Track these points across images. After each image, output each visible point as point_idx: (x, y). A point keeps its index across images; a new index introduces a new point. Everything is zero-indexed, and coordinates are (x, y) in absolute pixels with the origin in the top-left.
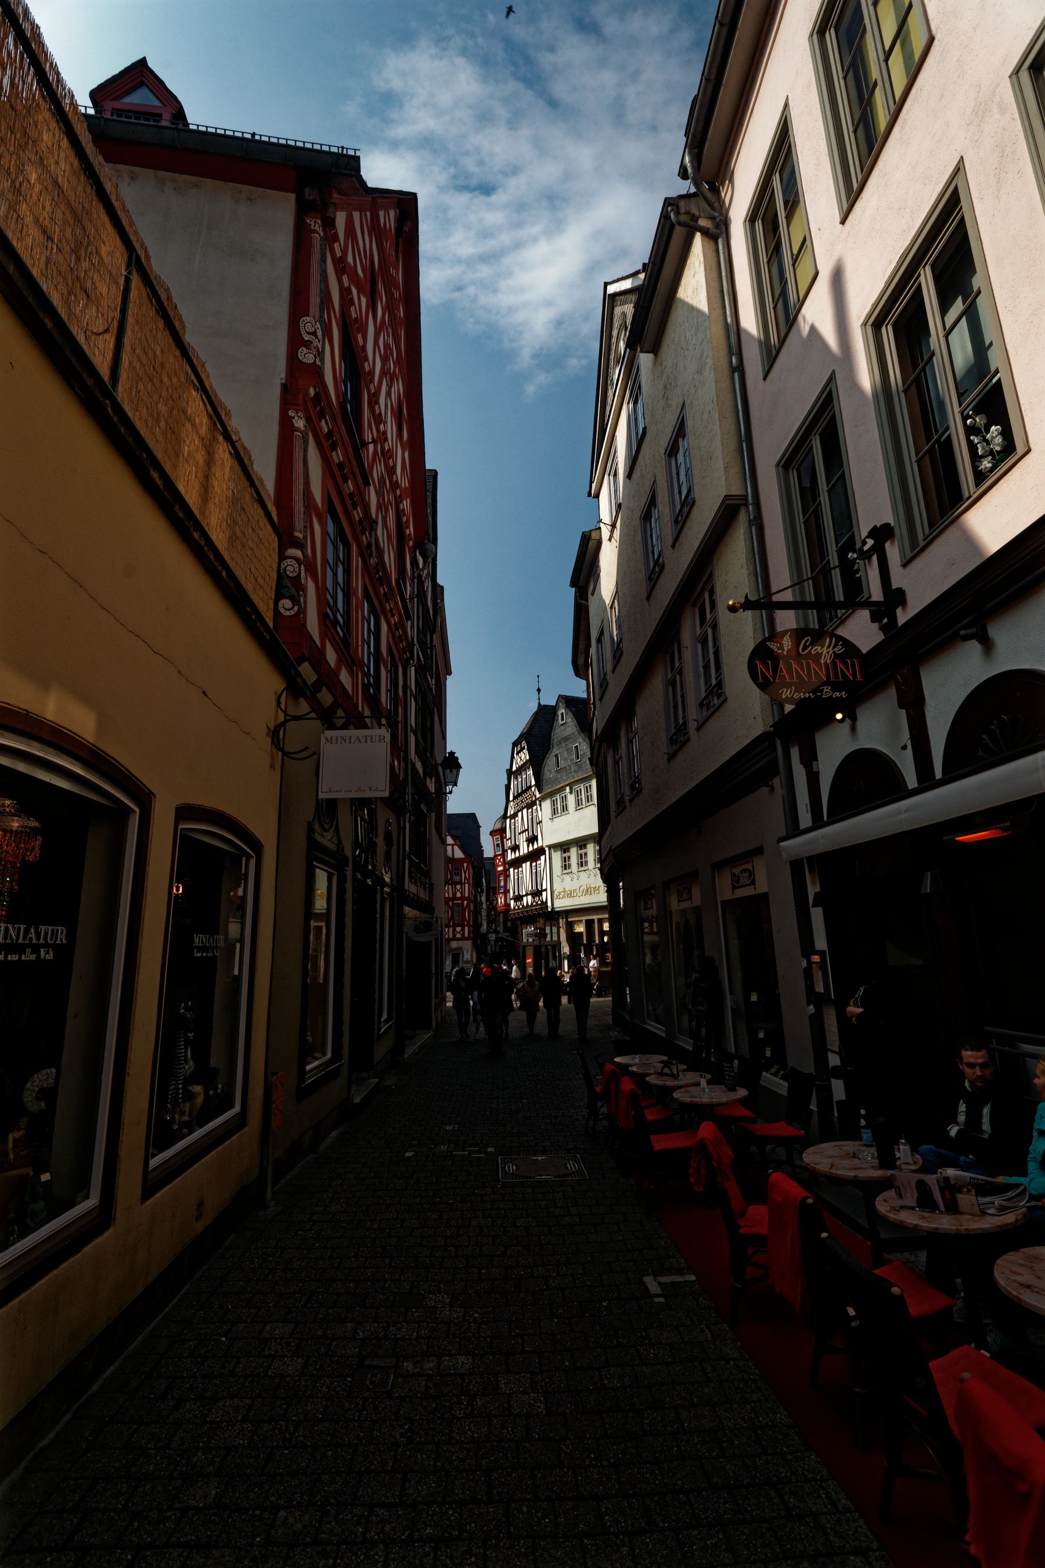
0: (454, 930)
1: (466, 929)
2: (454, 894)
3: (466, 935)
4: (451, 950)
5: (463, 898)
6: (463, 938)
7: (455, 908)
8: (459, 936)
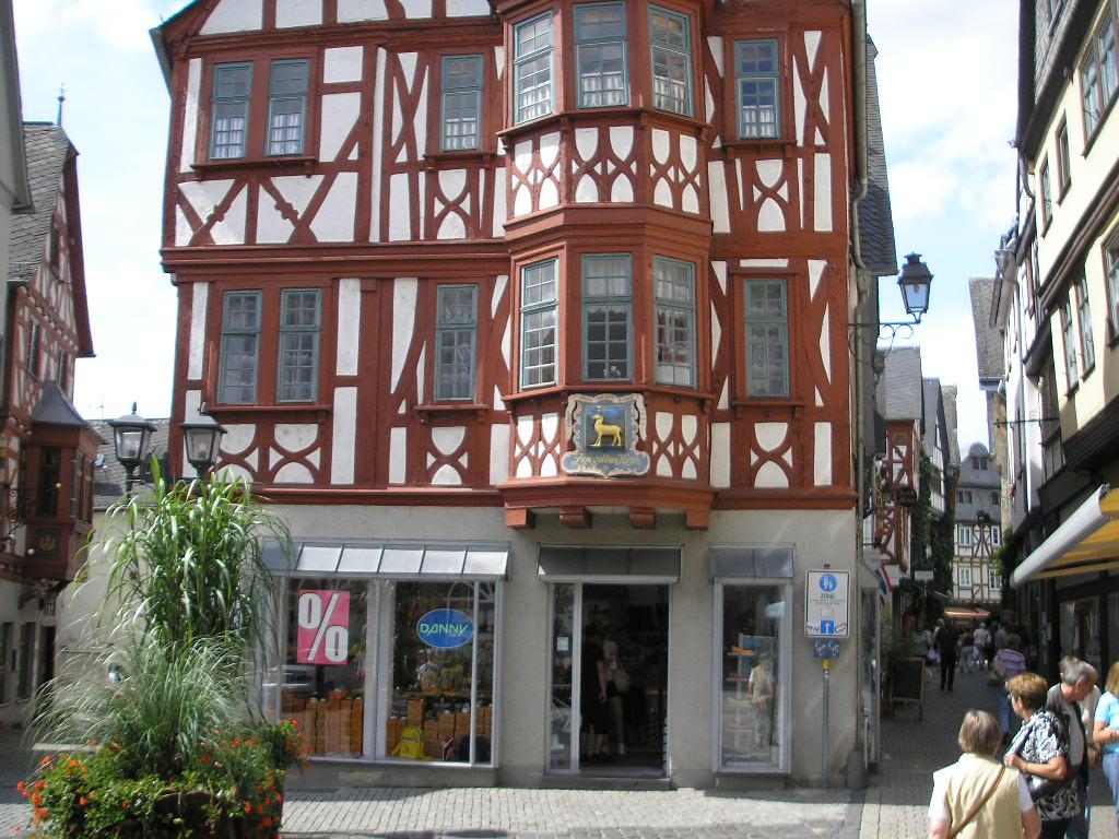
0: (743, 443)
1: (823, 433)
2: (744, 215)
3: (823, 474)
4: (720, 564)
5: (798, 241)
6: (801, 495)
7: (752, 308)
8: (771, 477)
